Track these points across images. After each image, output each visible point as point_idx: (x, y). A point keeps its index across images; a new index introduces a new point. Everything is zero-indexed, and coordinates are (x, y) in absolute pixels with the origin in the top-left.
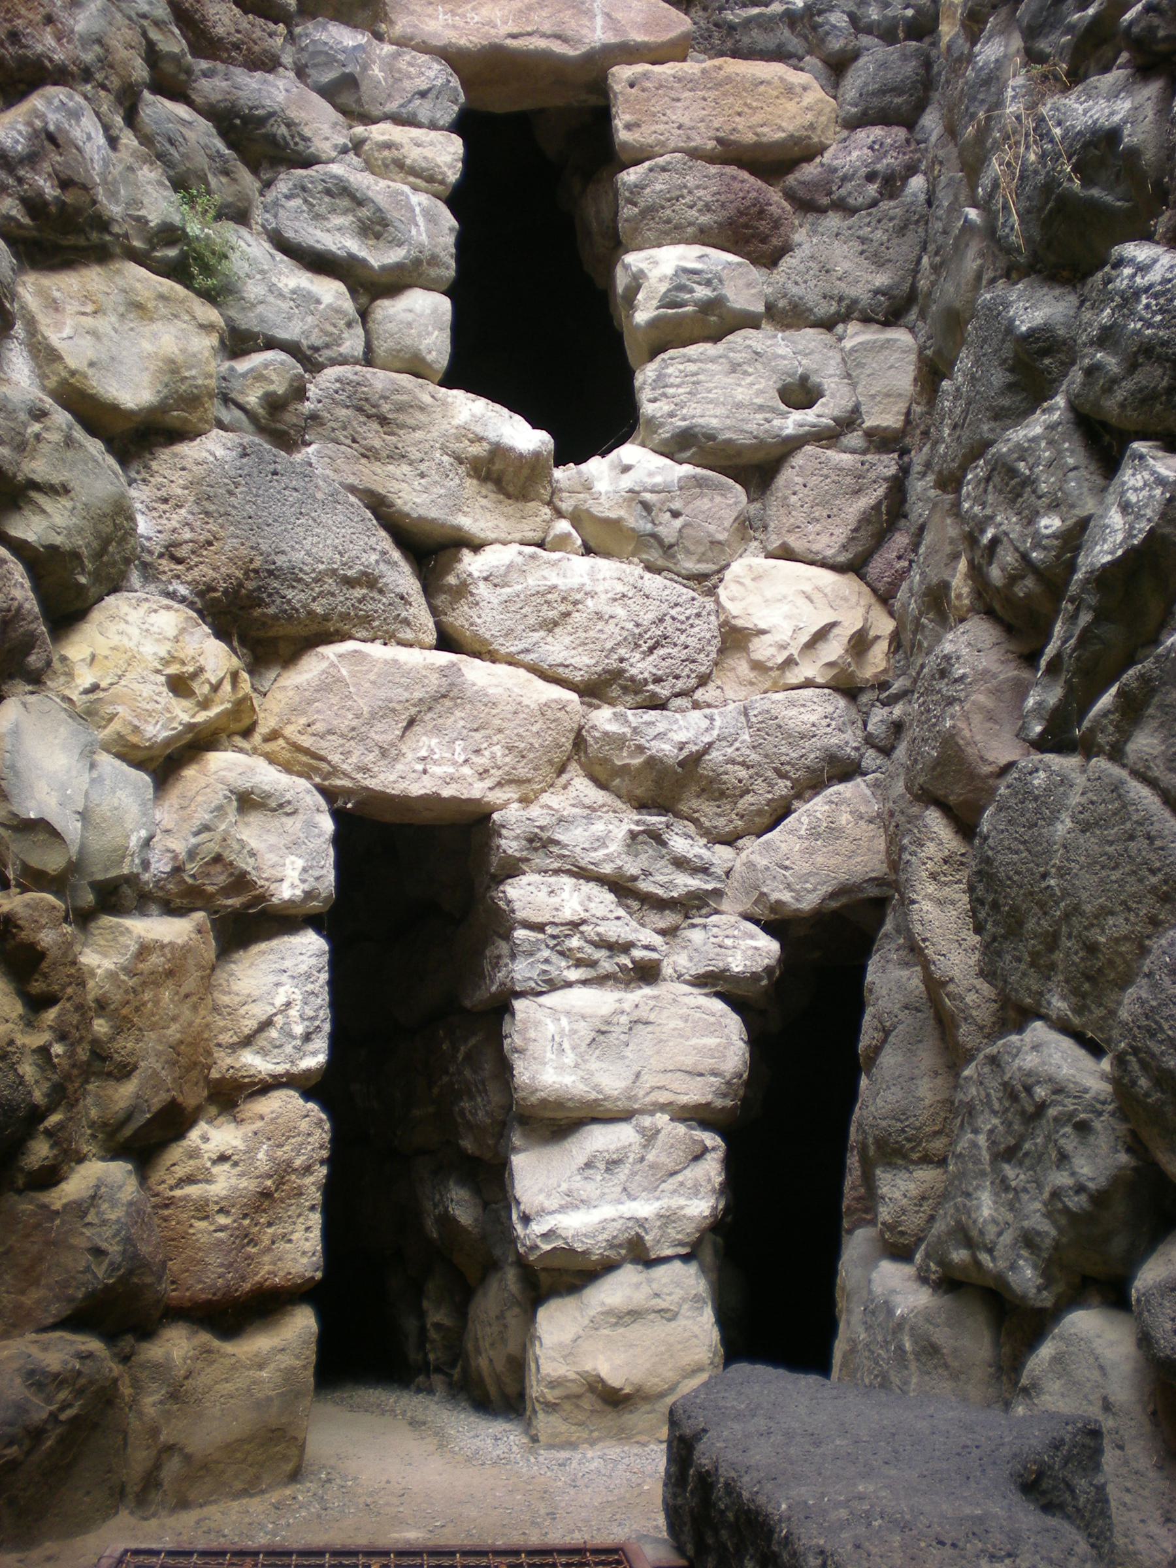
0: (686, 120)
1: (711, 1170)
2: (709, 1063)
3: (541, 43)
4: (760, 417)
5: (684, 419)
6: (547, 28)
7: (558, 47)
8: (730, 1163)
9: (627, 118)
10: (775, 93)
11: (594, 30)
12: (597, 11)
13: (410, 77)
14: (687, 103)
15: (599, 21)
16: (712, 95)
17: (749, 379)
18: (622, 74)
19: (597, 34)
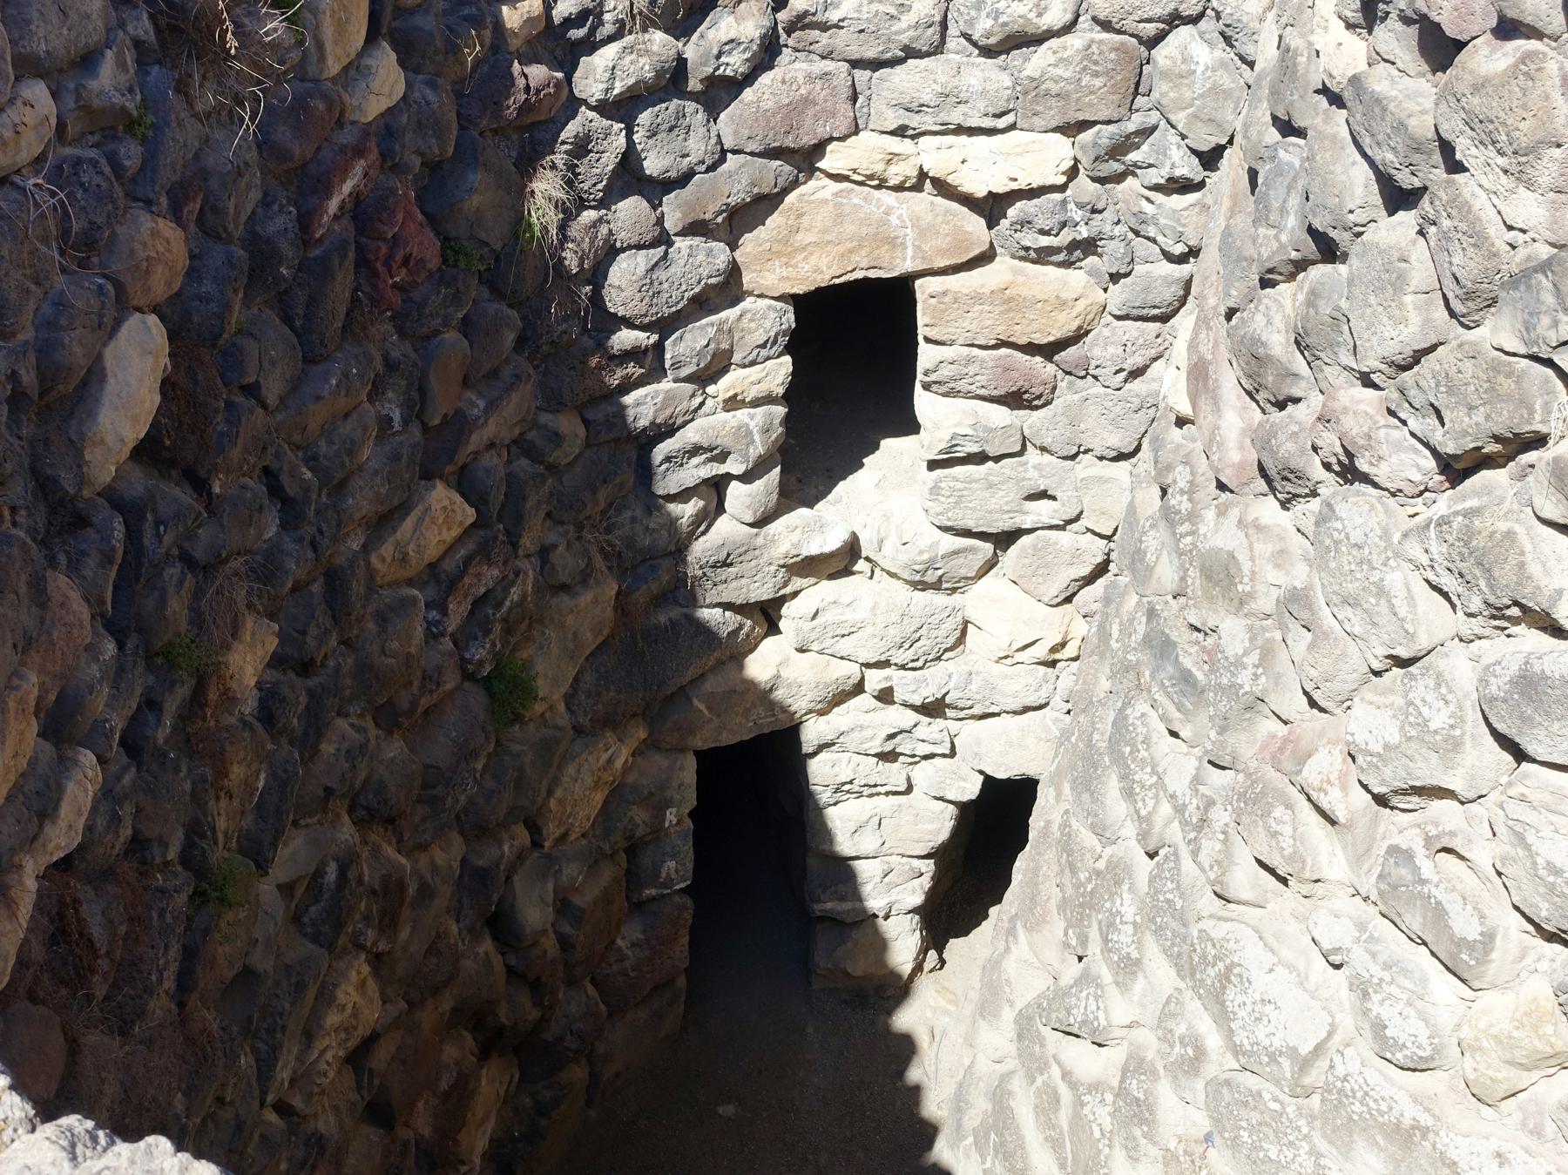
0: (973, 327)
1: (926, 882)
2: (927, 837)
3: (859, 275)
4: (1006, 516)
5: (949, 519)
6: (864, 264)
7: (873, 274)
8: (937, 879)
9: (927, 320)
10: (1049, 309)
11: (905, 259)
12: (909, 244)
13: (750, 332)
14: (975, 315)
15: (910, 252)
16: (998, 310)
17: (1002, 493)
18: (923, 287)
19: (908, 265)
